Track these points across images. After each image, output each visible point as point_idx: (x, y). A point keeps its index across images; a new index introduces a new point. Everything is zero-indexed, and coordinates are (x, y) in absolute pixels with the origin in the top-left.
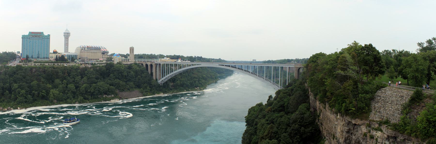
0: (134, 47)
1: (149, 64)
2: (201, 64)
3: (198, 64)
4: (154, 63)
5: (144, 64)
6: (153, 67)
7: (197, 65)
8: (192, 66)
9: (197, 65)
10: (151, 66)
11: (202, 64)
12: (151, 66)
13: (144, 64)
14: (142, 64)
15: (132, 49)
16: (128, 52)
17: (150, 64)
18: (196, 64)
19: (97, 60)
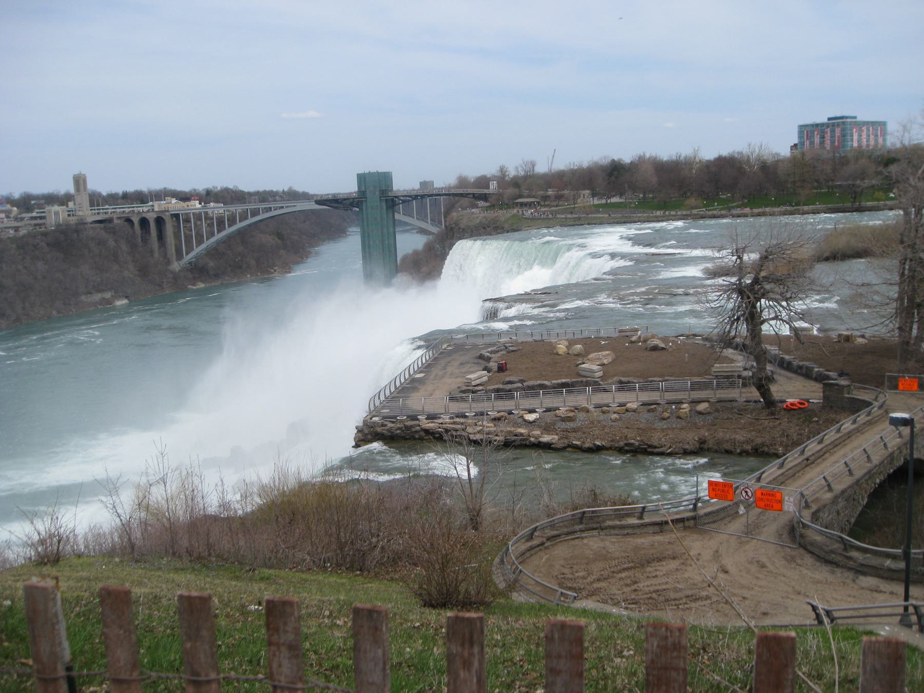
0: (86, 175)
1: (151, 217)
2: (295, 204)
3: (289, 205)
4: (167, 213)
5: (136, 220)
6: (167, 225)
7: (287, 207)
8: (275, 210)
9: (287, 207)
10: (160, 221)
11: (298, 204)
12: (160, 221)
13: (136, 220)
14: (129, 220)
15: (79, 181)
16: (72, 190)
17: (155, 216)
18: (283, 205)
19: (71, 213)
